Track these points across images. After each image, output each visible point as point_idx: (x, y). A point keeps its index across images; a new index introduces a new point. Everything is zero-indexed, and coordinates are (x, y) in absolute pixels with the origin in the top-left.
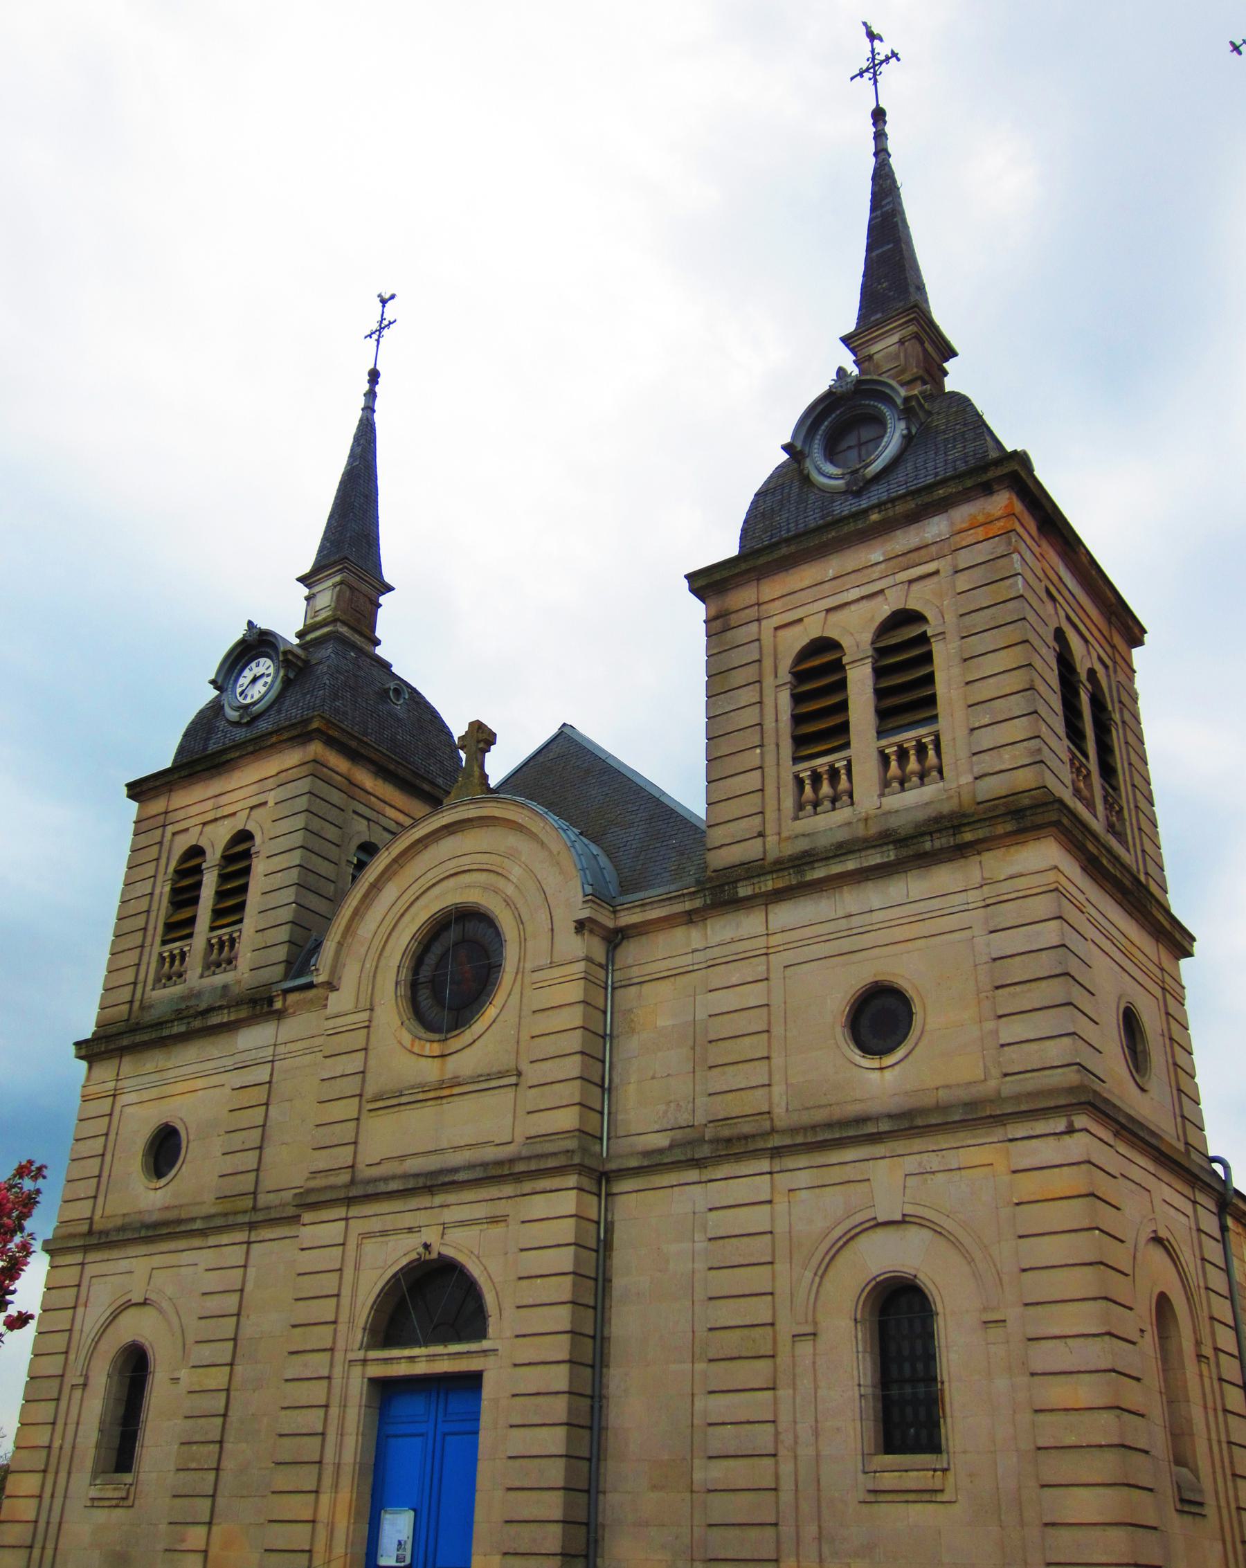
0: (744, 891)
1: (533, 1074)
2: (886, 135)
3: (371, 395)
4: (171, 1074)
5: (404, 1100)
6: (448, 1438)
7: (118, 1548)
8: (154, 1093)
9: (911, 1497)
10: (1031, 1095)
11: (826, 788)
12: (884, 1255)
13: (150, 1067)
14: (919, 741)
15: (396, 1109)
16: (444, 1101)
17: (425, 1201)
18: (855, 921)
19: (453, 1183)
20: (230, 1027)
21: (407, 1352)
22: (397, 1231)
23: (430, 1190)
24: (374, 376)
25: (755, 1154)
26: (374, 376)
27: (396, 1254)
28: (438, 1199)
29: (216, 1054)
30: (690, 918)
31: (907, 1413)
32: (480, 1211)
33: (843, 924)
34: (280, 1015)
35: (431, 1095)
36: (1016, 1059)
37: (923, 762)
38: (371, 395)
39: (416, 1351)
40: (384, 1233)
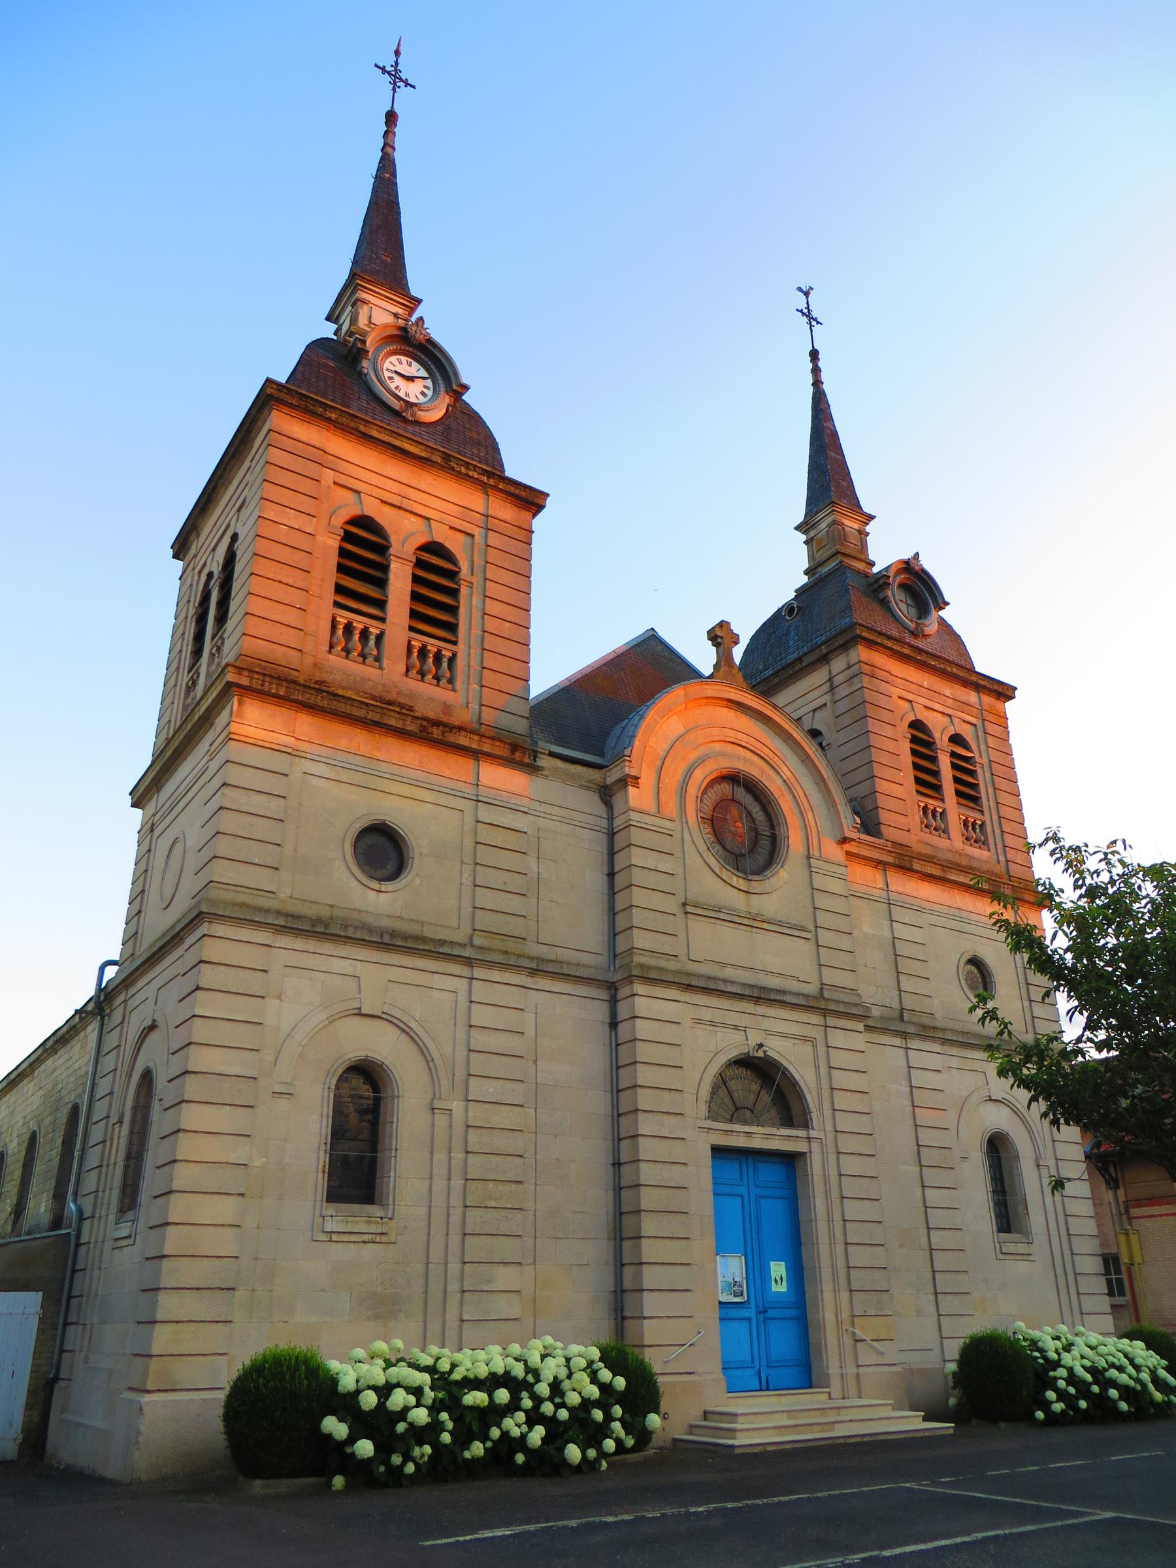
0: (917, 866)
1: (672, 905)
2: (394, 134)
3: (816, 371)
4: (383, 767)
5: (721, 916)
6: (739, 1200)
7: (379, 1289)
8: (357, 778)
9: (1019, 1257)
10: (243, 905)
11: (364, 645)
12: (380, 1044)
13: (343, 743)
14: (439, 651)
15: (714, 921)
16: (755, 930)
17: (749, 1007)
18: (964, 914)
19: (784, 1002)
20: (476, 755)
21: (746, 1129)
22: (726, 1025)
23: (757, 1000)
24: (814, 355)
25: (934, 1039)
26: (814, 355)
27: (733, 1045)
28: (761, 1009)
29: (447, 773)
30: (879, 864)
31: (356, 1169)
32: (794, 1029)
33: (957, 912)
34: (532, 769)
35: (746, 921)
36: (485, 921)
37: (434, 665)
38: (816, 371)
39: (754, 1129)
40: (713, 1024)
